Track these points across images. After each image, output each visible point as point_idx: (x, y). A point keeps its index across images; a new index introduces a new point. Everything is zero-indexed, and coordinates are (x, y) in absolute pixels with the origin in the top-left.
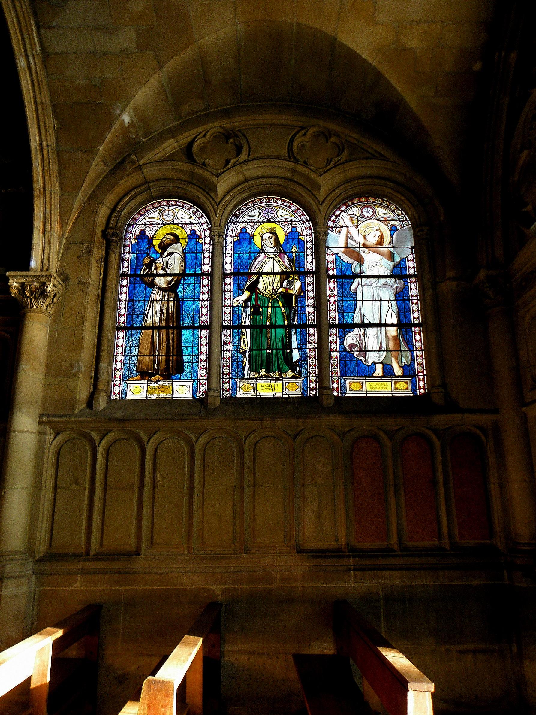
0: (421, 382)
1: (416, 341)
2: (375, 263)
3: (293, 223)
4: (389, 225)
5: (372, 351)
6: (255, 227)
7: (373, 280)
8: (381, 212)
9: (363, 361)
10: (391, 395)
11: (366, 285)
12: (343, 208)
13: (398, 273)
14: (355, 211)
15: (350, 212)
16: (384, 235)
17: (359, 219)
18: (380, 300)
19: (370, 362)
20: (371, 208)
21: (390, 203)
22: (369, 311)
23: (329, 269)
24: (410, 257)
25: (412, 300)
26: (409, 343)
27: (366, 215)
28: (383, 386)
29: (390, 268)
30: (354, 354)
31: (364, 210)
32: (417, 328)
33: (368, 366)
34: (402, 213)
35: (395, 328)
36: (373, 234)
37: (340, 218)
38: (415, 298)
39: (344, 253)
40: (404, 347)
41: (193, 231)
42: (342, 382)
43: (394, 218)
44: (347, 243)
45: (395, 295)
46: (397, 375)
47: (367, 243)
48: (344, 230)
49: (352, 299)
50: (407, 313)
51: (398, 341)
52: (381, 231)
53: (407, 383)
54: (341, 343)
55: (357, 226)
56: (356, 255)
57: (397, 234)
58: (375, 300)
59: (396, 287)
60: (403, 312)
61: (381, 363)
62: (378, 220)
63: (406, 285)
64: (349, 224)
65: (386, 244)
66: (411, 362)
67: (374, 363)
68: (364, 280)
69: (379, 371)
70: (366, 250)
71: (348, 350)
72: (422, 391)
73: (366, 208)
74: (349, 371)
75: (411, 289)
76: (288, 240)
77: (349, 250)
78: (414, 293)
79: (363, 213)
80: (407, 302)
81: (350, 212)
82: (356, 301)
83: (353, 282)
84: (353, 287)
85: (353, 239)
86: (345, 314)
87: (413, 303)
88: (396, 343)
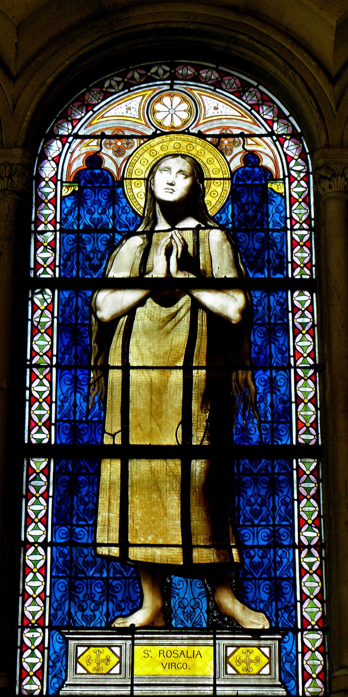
41: (251, 158)
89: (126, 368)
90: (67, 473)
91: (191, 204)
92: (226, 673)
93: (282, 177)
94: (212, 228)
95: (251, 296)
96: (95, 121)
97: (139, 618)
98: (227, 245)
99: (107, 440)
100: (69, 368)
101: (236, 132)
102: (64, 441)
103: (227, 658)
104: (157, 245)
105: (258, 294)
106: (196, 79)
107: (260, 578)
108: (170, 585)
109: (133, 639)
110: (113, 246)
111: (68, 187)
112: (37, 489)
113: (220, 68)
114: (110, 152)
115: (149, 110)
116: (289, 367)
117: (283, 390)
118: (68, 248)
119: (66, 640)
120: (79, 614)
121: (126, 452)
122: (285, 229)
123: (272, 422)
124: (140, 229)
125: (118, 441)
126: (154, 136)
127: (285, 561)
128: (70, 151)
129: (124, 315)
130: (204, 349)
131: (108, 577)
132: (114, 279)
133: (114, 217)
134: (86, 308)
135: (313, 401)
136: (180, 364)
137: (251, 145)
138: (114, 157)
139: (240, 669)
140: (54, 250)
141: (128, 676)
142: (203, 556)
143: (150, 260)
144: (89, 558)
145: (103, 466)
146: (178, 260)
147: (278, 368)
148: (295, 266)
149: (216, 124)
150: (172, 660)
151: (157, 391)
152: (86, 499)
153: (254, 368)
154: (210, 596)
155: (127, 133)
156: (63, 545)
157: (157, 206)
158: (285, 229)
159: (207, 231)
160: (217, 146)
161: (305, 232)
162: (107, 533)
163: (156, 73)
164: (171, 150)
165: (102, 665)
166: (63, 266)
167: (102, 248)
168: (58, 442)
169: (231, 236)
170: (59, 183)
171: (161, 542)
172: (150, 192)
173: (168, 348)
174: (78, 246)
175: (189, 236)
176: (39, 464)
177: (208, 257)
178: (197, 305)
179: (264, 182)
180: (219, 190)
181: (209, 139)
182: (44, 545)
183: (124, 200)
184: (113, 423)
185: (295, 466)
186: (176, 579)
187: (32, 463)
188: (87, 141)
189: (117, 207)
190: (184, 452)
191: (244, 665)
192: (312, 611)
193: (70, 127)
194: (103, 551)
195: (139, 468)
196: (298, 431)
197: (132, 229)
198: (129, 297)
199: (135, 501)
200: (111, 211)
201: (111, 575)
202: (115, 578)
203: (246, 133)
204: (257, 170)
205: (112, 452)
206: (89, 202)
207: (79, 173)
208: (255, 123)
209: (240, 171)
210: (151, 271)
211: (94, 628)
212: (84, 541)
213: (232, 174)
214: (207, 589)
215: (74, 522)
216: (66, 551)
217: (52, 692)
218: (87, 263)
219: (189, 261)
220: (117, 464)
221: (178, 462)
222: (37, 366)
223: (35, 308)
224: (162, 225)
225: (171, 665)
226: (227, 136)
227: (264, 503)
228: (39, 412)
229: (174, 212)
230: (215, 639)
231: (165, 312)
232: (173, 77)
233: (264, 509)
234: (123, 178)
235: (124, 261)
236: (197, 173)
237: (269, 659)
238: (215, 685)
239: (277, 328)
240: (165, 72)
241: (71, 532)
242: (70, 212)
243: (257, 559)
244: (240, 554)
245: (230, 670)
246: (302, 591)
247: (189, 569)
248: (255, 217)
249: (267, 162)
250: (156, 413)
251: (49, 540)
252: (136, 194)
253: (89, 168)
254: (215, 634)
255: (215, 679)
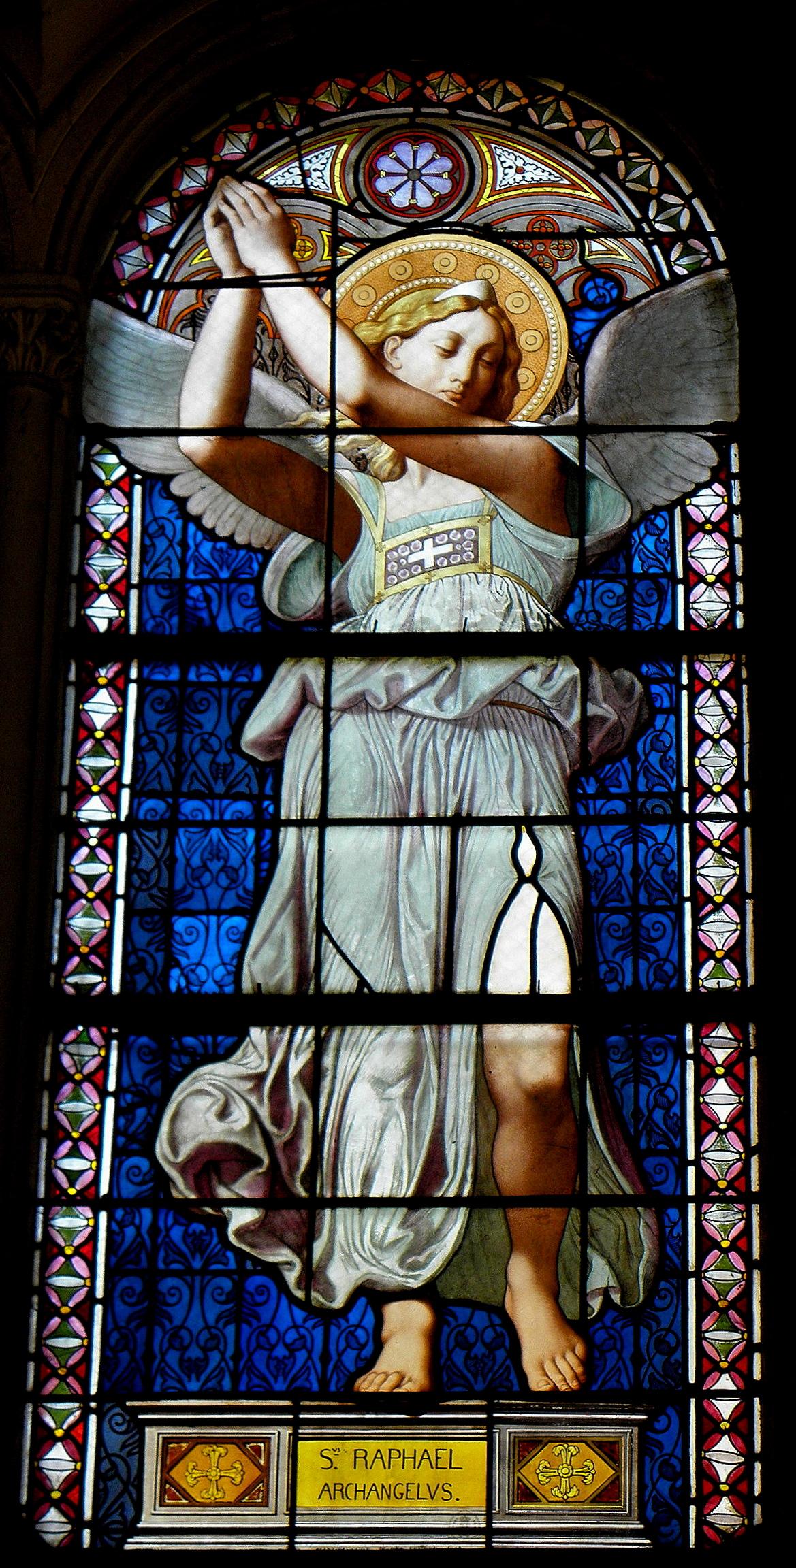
0: (725, 1444)
1: (706, 1123)
2: (435, 548)
4: (565, 267)
5: (363, 1203)
7: (411, 673)
8: (517, 172)
9: (291, 1277)
10: (477, 1542)
11: (359, 704)
12: (233, 149)
13: (605, 621)
14: (324, 168)
15: (287, 177)
16: (526, 340)
17: (349, 224)
18: (459, 822)
19: (342, 1279)
20: (443, 150)
21: (582, 113)
22: (369, 901)
23: (89, 592)
24: (708, 504)
25: (694, 818)
26: (653, 1149)
27: (401, 199)
28: (425, 1475)
29: (548, 581)
30: (224, 1222)
31: (385, 164)
32: (723, 1031)
33: (328, 1317)
34: (667, 184)
35: (550, 1032)
36: (437, 334)
37: (208, 218)
38: (726, 805)
39: (212, 469)
40: (606, 1174)
42: (114, 1442)
43: (603, 216)
44: (238, 394)
45: (572, 784)
46: (537, 1383)
47: (391, 397)
48: (228, 306)
49: (244, 807)
50: (649, 919)
51: (565, 1132)
52: (500, 316)
53: (609, 1450)
54: (136, 1139)
55: (321, 282)
56: (303, 485)
57: (621, 336)
58: (422, 820)
59: (586, 722)
60: (617, 913)
61: (427, 1293)
62: (487, 232)
63: (651, 715)
64: (267, 260)
65: (528, 408)
66: (652, 1290)
67: (373, 1297)
68: (347, 672)
69: (403, 1356)
70: (383, 453)
71: (183, 1189)
72: (724, 1512)
73: (404, 151)
74: (173, 1358)
75: (698, 736)
77: (254, 453)
78: (718, 763)
79: (382, 185)
80: (660, 832)
81: (287, 177)
82: (278, 823)
83: (259, 690)
84: (258, 725)
85: (285, 365)
86: (180, 924)
87: (700, 843)
88: (550, 1144)
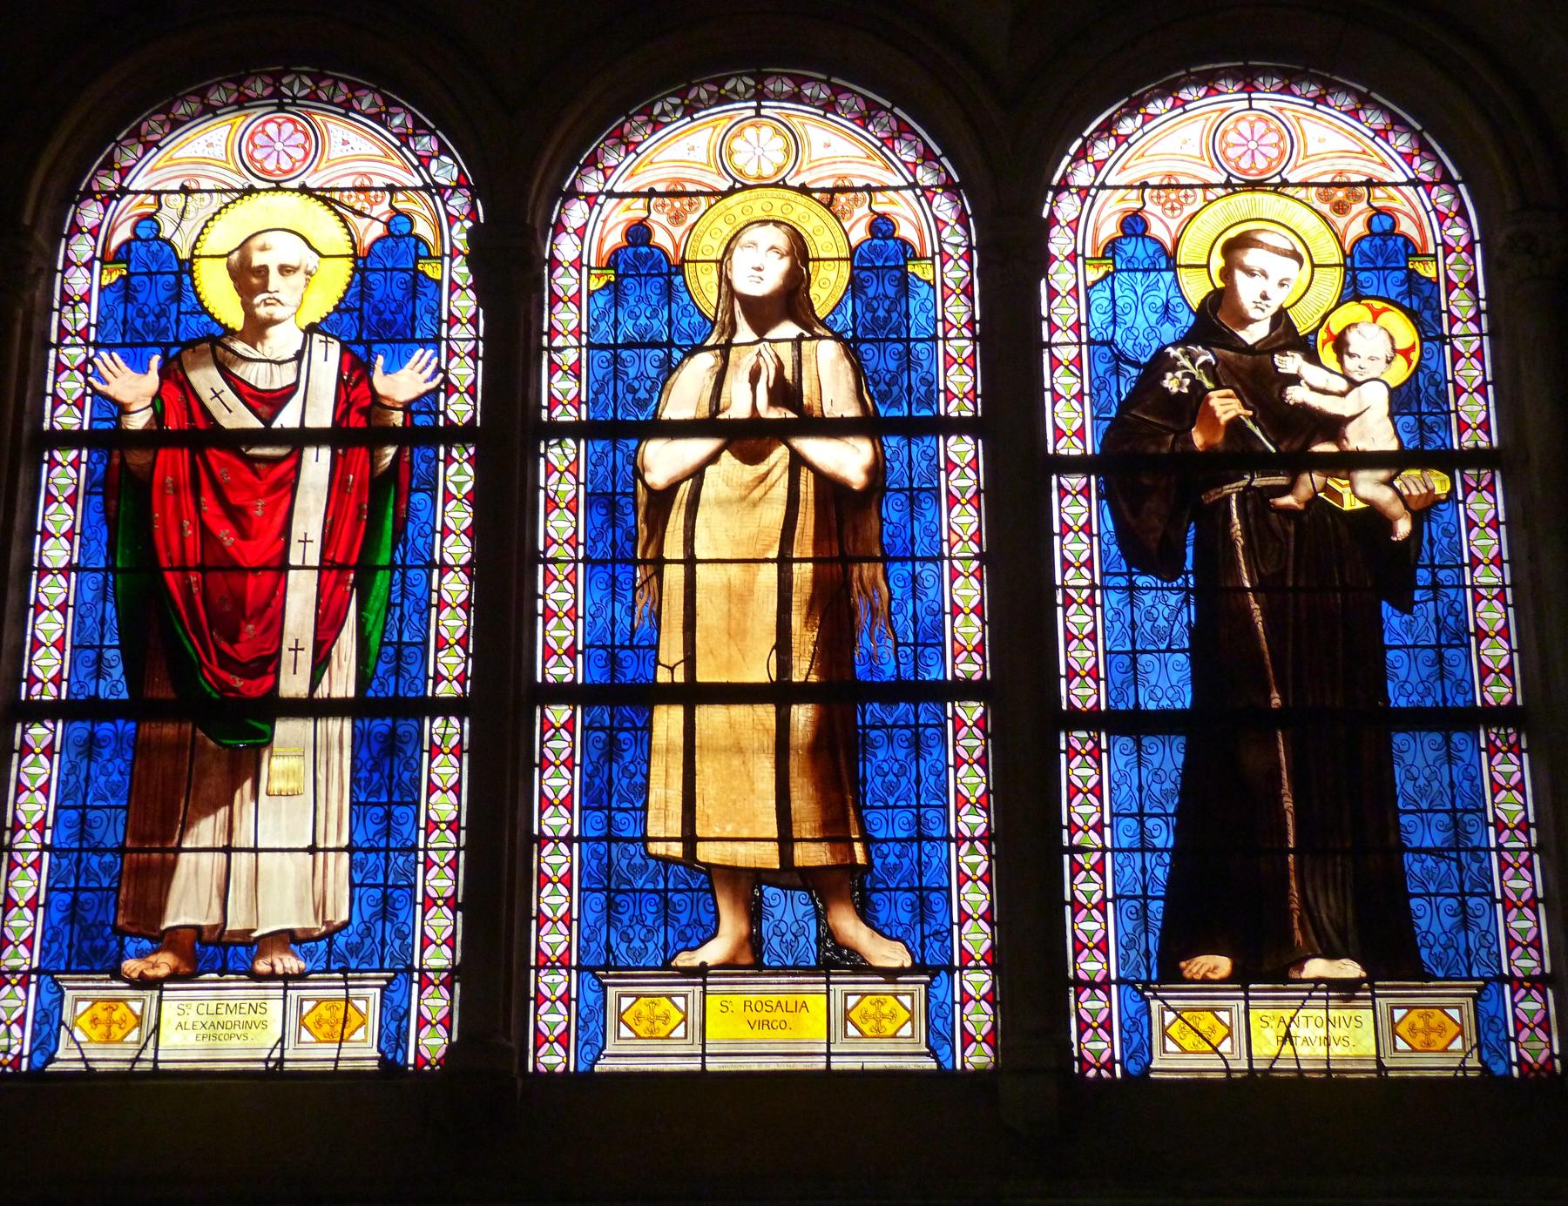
3: (1378, 192)
6: (1188, 211)
41: (881, 226)
76: (1354, 278)
89: (690, 562)
90: (602, 729)
91: (791, 299)
92: (846, 1035)
93: (929, 254)
94: (820, 337)
95: (882, 445)
96: (640, 169)
97: (714, 952)
98: (845, 365)
99: (663, 676)
100: (603, 562)
101: (859, 183)
102: (597, 679)
103: (846, 1012)
104: (737, 366)
105: (893, 441)
106: (796, 98)
107: (897, 889)
108: (760, 901)
109: (704, 984)
110: (669, 369)
111: (598, 277)
112: (557, 754)
113: (834, 80)
114: (663, 219)
115: (722, 154)
116: (941, 557)
117: (931, 593)
118: (600, 373)
119: (604, 987)
120: (623, 946)
121: (692, 694)
122: (934, 338)
123: (916, 644)
124: (710, 342)
125: (679, 677)
126: (732, 191)
127: (935, 861)
128: (602, 217)
129: (687, 479)
130: (810, 531)
131: (666, 890)
132: (670, 421)
133: (670, 322)
134: (629, 468)
135: (978, 610)
136: (774, 554)
137: (882, 203)
138: (670, 227)
139: (865, 1028)
140: (578, 377)
141: (698, 1040)
142: (810, 855)
143: (725, 390)
144: (638, 860)
145: (656, 716)
146: (771, 392)
147: (924, 560)
148: (950, 396)
149: (826, 171)
150: (764, 1016)
151: (739, 598)
152: (632, 768)
153: (886, 559)
154: (821, 916)
155: (690, 188)
156: (598, 840)
157: (737, 303)
158: (934, 338)
159: (814, 342)
160: (828, 206)
161: (966, 343)
162: (664, 821)
163: (734, 90)
164: (761, 215)
165: (658, 1024)
166: (593, 402)
167: (653, 373)
168: (588, 681)
169: (852, 349)
170: (585, 270)
171: (745, 834)
172: (725, 280)
173: (754, 530)
174: (616, 369)
175: (785, 352)
176: (559, 714)
177: (815, 384)
178: (798, 462)
179: (902, 262)
180: (832, 276)
181: (817, 195)
182: (569, 840)
183: (685, 296)
184: (671, 648)
185: (950, 714)
186: (769, 891)
187: (548, 712)
188: (628, 201)
189: (674, 306)
190: (780, 693)
191: (872, 1023)
192: (976, 938)
193: (601, 179)
194: (657, 848)
195: (711, 717)
196: (954, 658)
197: (698, 341)
198: (697, 449)
199: (705, 768)
200: (666, 313)
201: (670, 886)
202: (677, 891)
203: (874, 184)
204: (891, 243)
205: (670, 694)
206: (631, 299)
207: (615, 252)
208: (887, 168)
209: (865, 246)
210: (727, 408)
211: (645, 968)
212: (628, 834)
213: (853, 251)
214: (816, 906)
215: (614, 805)
216: (602, 849)
217: (582, 1067)
218: (629, 397)
219: (786, 392)
220: (677, 712)
221: (771, 709)
222: (555, 561)
223: (550, 469)
224: (745, 333)
225: (763, 1024)
226: (844, 190)
227: (903, 771)
228: (557, 633)
229: (763, 313)
230: (828, 983)
231: (750, 472)
232: (760, 96)
233: (904, 781)
234: (683, 260)
235: (685, 395)
236: (799, 251)
237: (911, 1013)
238: (829, 1054)
239: (921, 497)
240: (747, 87)
241: (610, 818)
242: (603, 315)
243: (892, 859)
244: (867, 853)
245: (852, 1031)
246: (960, 908)
247: (789, 876)
248: (887, 320)
249: (906, 231)
250: (736, 633)
251: (576, 833)
252: (704, 286)
253: (631, 245)
254: (828, 975)
255: (829, 1044)
